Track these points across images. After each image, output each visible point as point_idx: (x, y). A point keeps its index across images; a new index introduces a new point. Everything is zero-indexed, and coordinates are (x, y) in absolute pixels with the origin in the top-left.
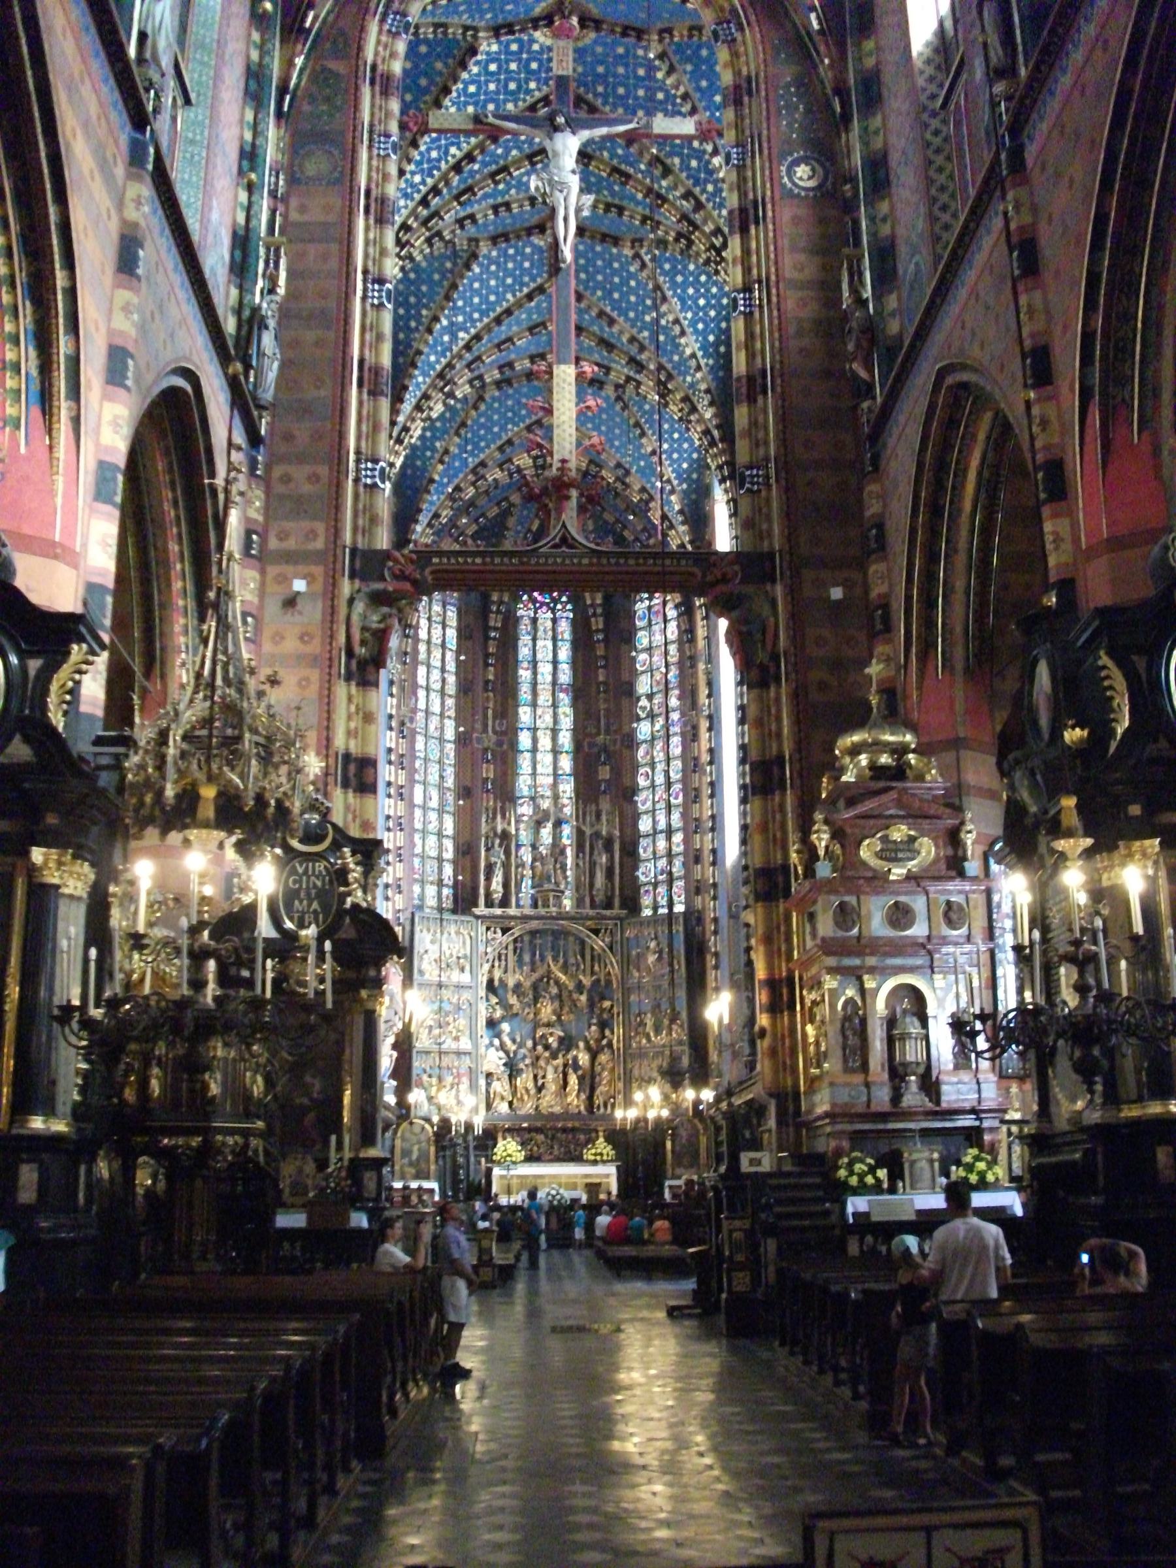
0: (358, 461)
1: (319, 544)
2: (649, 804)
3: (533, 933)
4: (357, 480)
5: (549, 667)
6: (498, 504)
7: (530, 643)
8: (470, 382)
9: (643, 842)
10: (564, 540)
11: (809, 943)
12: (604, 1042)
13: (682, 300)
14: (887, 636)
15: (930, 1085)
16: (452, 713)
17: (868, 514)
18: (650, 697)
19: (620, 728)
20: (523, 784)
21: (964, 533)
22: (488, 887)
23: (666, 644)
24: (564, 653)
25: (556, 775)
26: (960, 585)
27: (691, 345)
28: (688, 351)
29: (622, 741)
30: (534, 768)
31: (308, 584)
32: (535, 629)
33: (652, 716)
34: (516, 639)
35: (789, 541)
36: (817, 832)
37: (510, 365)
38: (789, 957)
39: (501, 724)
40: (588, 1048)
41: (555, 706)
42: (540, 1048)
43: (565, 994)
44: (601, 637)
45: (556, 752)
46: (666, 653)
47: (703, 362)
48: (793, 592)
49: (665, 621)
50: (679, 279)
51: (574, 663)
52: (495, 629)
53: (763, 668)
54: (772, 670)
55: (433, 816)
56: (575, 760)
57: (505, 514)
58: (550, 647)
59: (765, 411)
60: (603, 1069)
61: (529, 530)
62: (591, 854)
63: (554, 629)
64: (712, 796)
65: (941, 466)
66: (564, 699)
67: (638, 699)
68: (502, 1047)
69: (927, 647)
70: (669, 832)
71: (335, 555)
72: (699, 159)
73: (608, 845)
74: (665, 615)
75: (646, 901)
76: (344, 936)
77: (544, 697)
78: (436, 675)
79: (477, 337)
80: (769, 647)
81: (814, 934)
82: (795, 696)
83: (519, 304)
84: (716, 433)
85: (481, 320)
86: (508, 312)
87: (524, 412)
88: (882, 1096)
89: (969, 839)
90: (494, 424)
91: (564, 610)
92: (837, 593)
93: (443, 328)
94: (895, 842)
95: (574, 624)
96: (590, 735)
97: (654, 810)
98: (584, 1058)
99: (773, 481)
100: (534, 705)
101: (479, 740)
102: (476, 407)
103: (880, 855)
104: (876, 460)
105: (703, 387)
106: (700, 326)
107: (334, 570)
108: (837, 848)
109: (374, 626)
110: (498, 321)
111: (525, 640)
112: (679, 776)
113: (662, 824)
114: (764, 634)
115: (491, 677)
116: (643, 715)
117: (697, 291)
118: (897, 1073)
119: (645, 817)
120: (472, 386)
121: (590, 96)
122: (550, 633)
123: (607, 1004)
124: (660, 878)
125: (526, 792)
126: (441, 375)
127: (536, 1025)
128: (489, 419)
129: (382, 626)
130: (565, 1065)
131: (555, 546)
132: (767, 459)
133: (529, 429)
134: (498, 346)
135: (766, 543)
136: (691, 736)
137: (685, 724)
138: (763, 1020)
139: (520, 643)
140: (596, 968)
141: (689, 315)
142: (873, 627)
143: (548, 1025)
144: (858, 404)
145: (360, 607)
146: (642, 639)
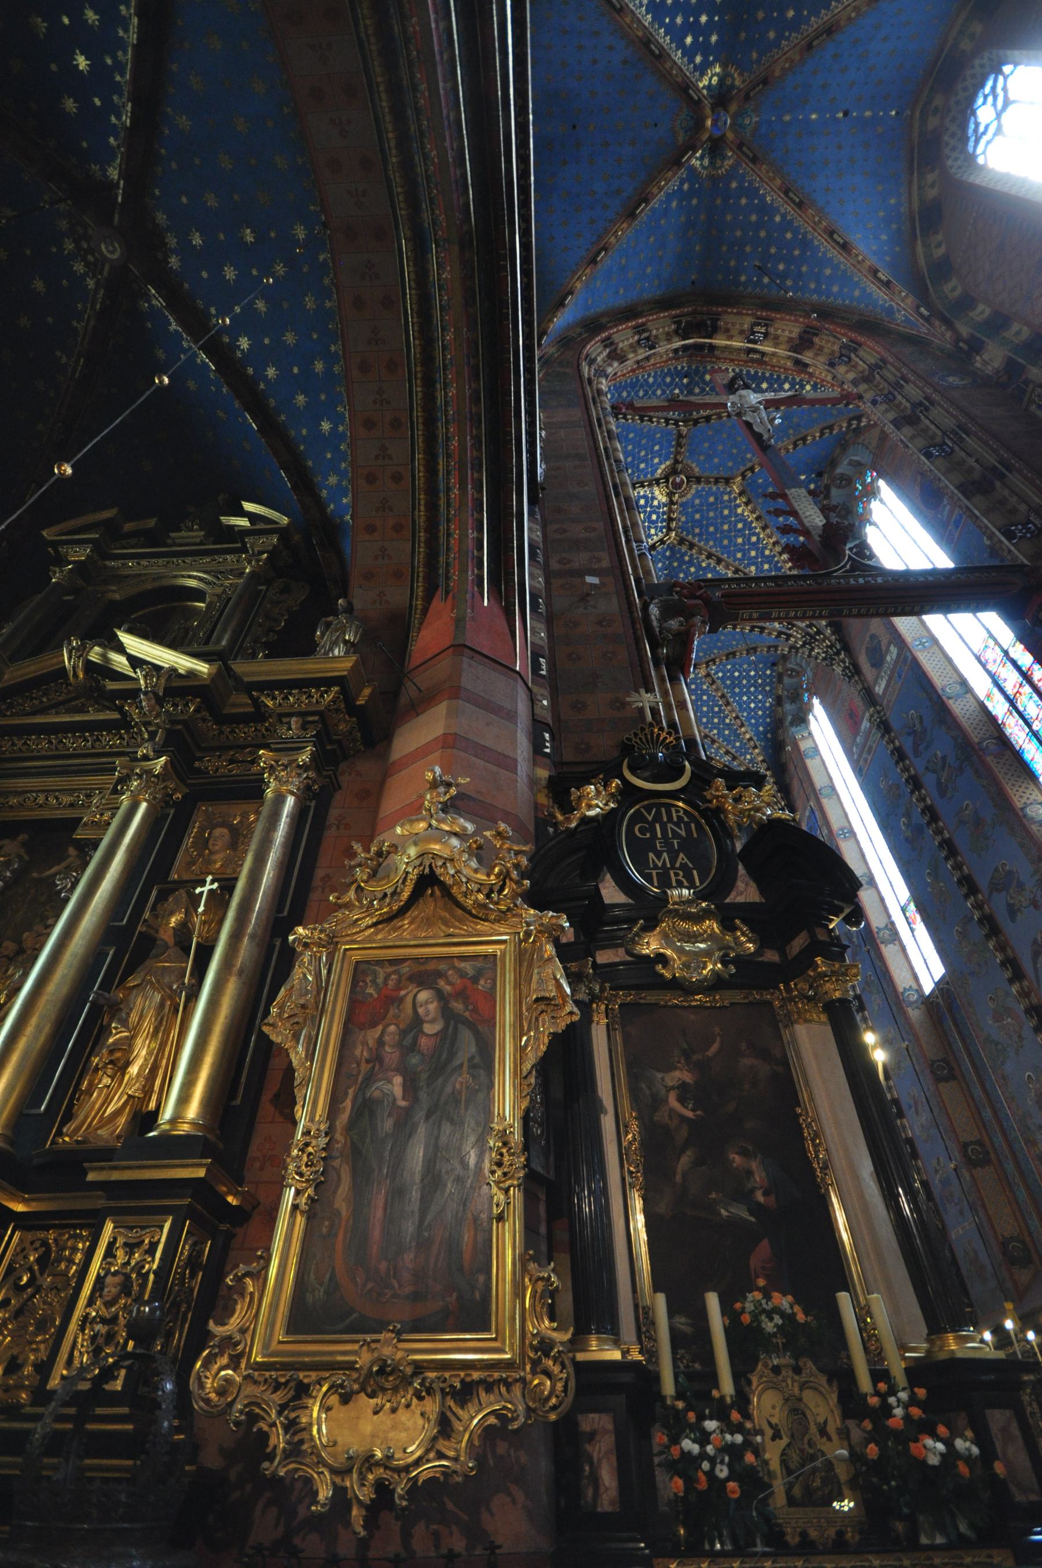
28: (748, 736)
47: (758, 743)
50: (737, 690)
72: (770, 563)
76: (741, 899)
105: (761, 758)
117: (749, 698)
121: (690, 537)
131: (845, 572)
141: (745, 714)
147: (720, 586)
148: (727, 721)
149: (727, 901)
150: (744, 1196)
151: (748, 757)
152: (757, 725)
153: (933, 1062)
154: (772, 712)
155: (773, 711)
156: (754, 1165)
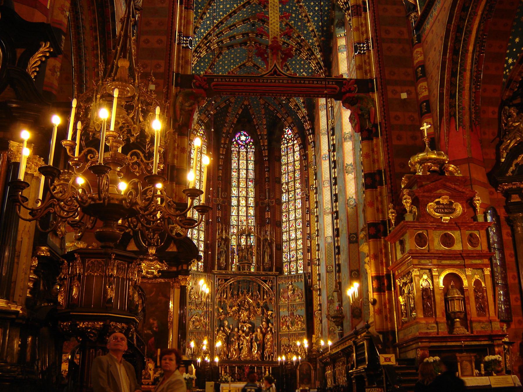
0: (180, 36)
1: (162, 70)
3: (239, 282)
4: (179, 44)
5: (245, 171)
6: (225, 102)
7: (237, 161)
8: (217, 43)
9: (284, 244)
10: (275, 72)
11: (399, 256)
12: (269, 329)
13: (309, 9)
14: (429, 114)
15: (466, 322)
17: (416, 62)
18: (287, 184)
19: (275, 196)
20: (233, 220)
21: (469, 61)
22: (219, 259)
23: (294, 161)
24: (251, 166)
25: (247, 216)
26: (467, 85)
27: (311, 26)
28: (311, 29)
29: (276, 202)
30: (238, 213)
31: (156, 87)
32: (239, 155)
33: (288, 191)
34: (231, 160)
35: (380, 73)
36: (405, 199)
37: (234, 37)
38: (387, 265)
39: (224, 194)
40: (262, 332)
41: (247, 187)
42: (240, 332)
43: (251, 308)
44: (266, 159)
45: (247, 206)
46: (294, 165)
47: (317, 34)
48: (383, 95)
49: (294, 152)
51: (255, 171)
52: (223, 155)
53: (369, 131)
54: (374, 131)
56: (255, 210)
57: (228, 106)
58: (245, 163)
59: (366, 19)
60: (268, 341)
61: (238, 114)
63: (247, 156)
64: (317, 221)
65: (459, 30)
66: (251, 185)
67: (282, 184)
68: (224, 331)
69: (452, 116)
70: (296, 239)
71: (169, 75)
73: (270, 245)
74: (294, 150)
75: (286, 269)
76: (170, 250)
77: (242, 184)
79: (222, 23)
80: (372, 121)
81: (403, 250)
82: (387, 141)
83: (239, 9)
84: (322, 64)
85: (223, 15)
86: (235, 12)
87: (238, 60)
88: (443, 329)
89: (478, 203)
90: (225, 65)
91: (251, 148)
92: (404, 96)
93: (207, 18)
94: (443, 204)
95: (255, 154)
96: (262, 199)
97: (289, 231)
98: (260, 336)
99: (371, 48)
100: (238, 187)
101: (216, 201)
102: (218, 57)
103: (436, 210)
104: (419, 38)
105: (317, 44)
106: (316, 19)
107: (168, 82)
108: (415, 209)
109: (187, 108)
110: (230, 16)
111: (234, 159)
112: (300, 216)
113: (293, 236)
114: (369, 115)
115: (221, 175)
116: (284, 191)
118: (450, 317)
120: (218, 45)
122: (245, 157)
123: (270, 313)
124: (292, 259)
125: (235, 223)
126: (206, 38)
127: (239, 321)
128: (224, 62)
129: (190, 108)
130: (252, 339)
131: (270, 75)
132: (367, 39)
133: (240, 67)
134: (230, 27)
135: (369, 75)
136: (306, 198)
137: (303, 194)
138: (372, 296)
139: (233, 161)
140: (265, 297)
141: (311, 14)
142: (421, 110)
143: (244, 322)
144: (409, 15)
145: (180, 99)
146: (284, 160)
147: (213, 79)
148: (300, 17)
149: (167, 251)
150: (151, 328)
151: (311, 41)
152: (317, 21)
153: (351, 234)
154: (328, 13)
155: (330, 13)
156: (155, 322)
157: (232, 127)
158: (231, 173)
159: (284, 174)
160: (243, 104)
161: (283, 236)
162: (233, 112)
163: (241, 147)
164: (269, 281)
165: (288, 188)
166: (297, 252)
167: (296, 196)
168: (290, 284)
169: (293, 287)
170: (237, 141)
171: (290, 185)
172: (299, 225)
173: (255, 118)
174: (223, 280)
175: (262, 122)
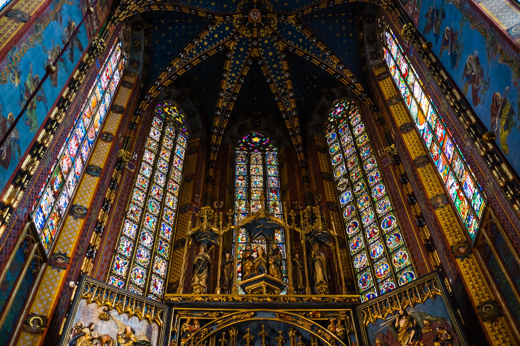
2: (362, 245)
16: (176, 192)
24: (272, 172)
52: (216, 146)
55: (144, 253)
61: (242, 76)
62: (309, 254)
63: (263, 159)
67: (338, 181)
70: (388, 254)
78: (163, 164)
91: (271, 150)
97: (367, 247)
100: (249, 199)
113: (379, 250)
119: (359, 256)
139: (237, 167)
157: (232, 100)
158: (234, 181)
159: (337, 166)
160: (250, 57)
161: (355, 262)
162: (233, 75)
163: (252, 150)
164: (335, 322)
165: (350, 181)
166: (397, 279)
167: (370, 182)
168: (400, 317)
169: (411, 319)
170: (245, 144)
171: (354, 174)
172: (389, 224)
173: (272, 82)
174: (196, 322)
175: (286, 89)
